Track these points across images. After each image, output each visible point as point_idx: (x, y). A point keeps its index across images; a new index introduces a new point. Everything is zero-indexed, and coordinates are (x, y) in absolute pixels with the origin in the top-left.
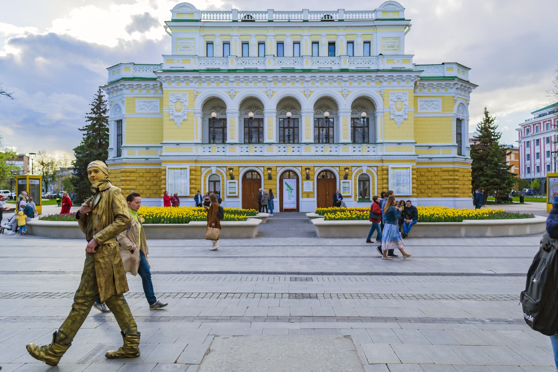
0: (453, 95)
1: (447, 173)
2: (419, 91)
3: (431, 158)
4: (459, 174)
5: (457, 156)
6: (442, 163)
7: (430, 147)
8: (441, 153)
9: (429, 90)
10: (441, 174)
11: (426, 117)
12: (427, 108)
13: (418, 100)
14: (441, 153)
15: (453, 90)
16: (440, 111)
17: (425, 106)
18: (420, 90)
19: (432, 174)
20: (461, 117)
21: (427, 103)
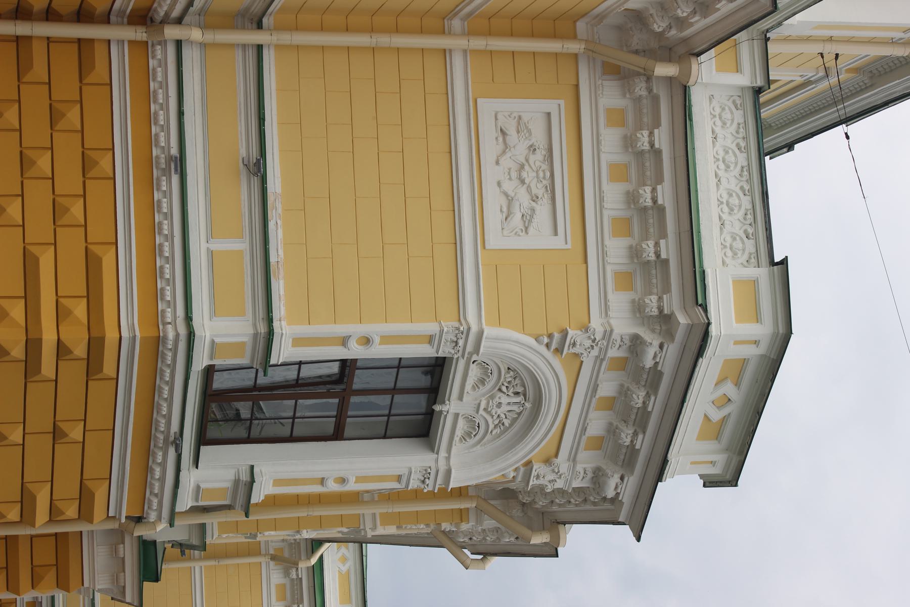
0: (597, 324)
1: (75, 283)
2: (609, 111)
3: (180, 163)
4: (73, 373)
5: (201, 361)
6: (150, 251)
7: (258, 168)
8: (218, 246)
9: (618, 173)
10: (72, 244)
11: (451, 152)
12: (506, 162)
13: (551, 105)
14: (218, 246)
15: (623, 326)
16: (494, 241)
17: (520, 150)
18: (616, 118)
19: (69, 180)
20: (454, 407)
21: (539, 156)
